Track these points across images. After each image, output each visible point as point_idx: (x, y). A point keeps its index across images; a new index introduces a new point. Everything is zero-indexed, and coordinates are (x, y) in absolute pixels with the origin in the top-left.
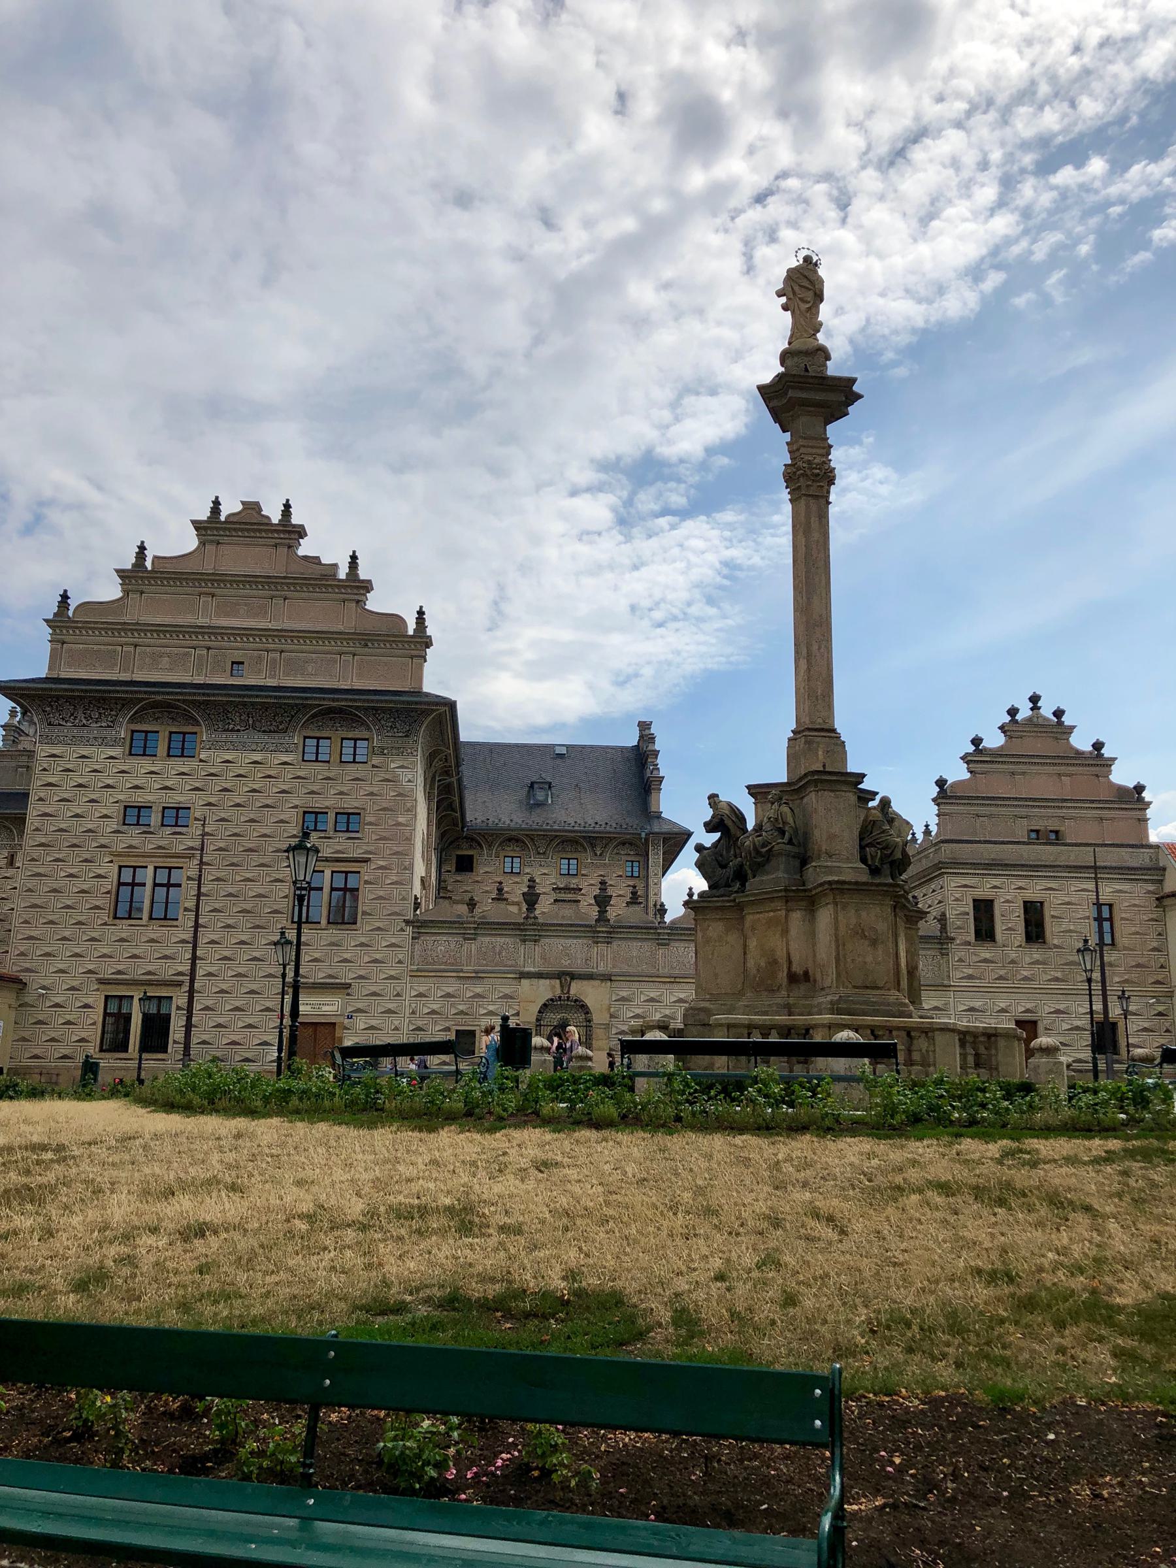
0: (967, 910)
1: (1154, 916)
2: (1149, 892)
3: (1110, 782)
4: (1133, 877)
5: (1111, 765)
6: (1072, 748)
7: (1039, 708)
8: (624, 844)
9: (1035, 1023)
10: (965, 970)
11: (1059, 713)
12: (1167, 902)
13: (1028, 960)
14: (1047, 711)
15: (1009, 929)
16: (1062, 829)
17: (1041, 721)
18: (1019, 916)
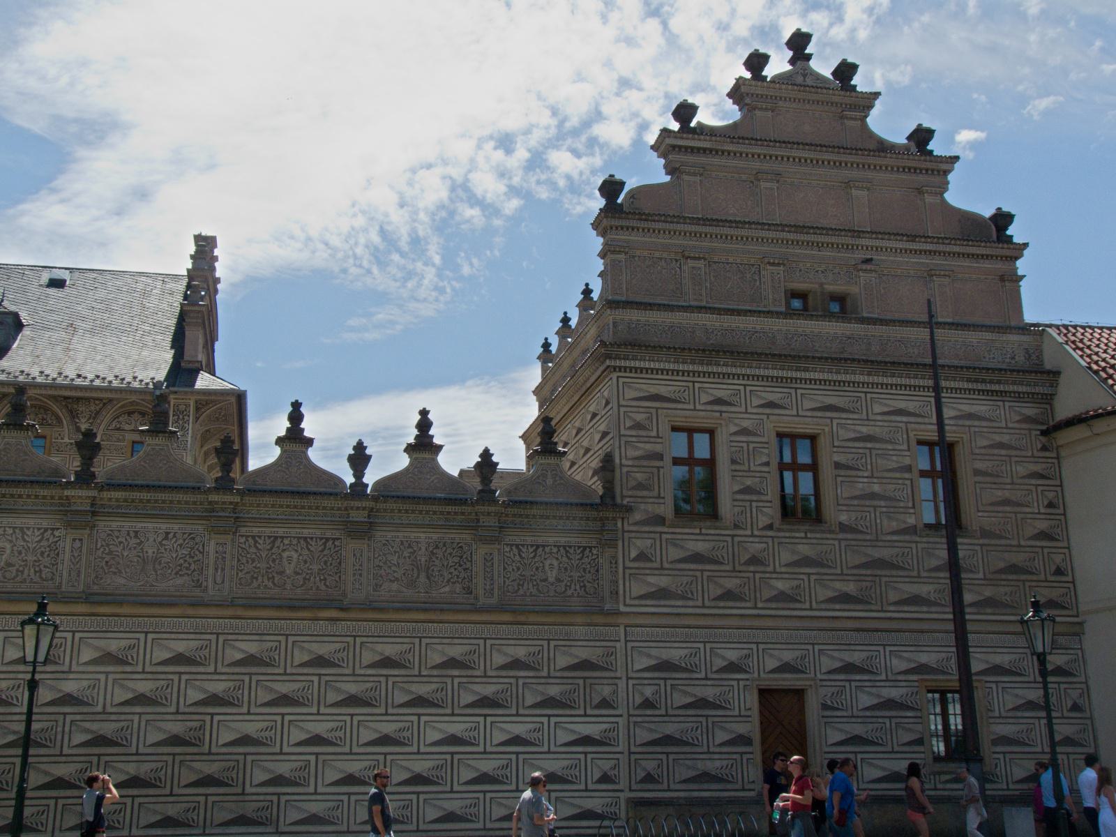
0: (658, 448)
1: (1038, 468)
2: (1027, 420)
3: (944, 202)
4: (995, 387)
5: (946, 172)
6: (871, 135)
7: (808, 57)
8: (130, 413)
9: (799, 693)
10: (651, 579)
11: (845, 71)
12: (1064, 437)
13: (786, 557)
14: (823, 67)
15: (747, 490)
16: (854, 289)
17: (809, 81)
18: (767, 464)
